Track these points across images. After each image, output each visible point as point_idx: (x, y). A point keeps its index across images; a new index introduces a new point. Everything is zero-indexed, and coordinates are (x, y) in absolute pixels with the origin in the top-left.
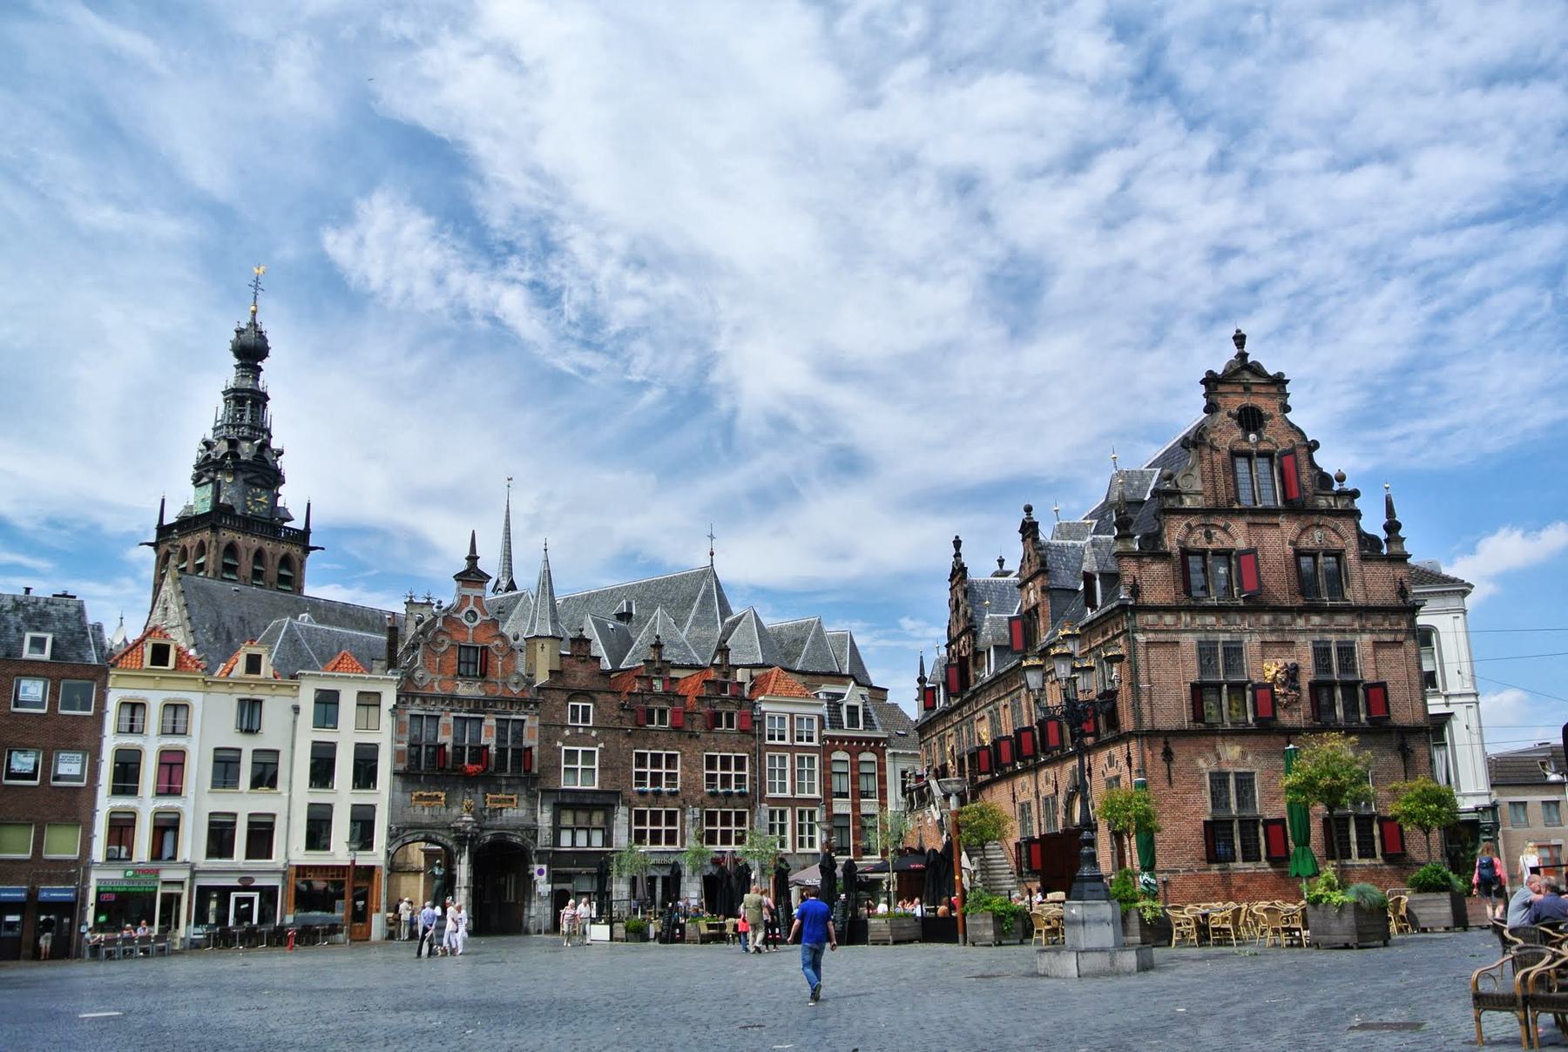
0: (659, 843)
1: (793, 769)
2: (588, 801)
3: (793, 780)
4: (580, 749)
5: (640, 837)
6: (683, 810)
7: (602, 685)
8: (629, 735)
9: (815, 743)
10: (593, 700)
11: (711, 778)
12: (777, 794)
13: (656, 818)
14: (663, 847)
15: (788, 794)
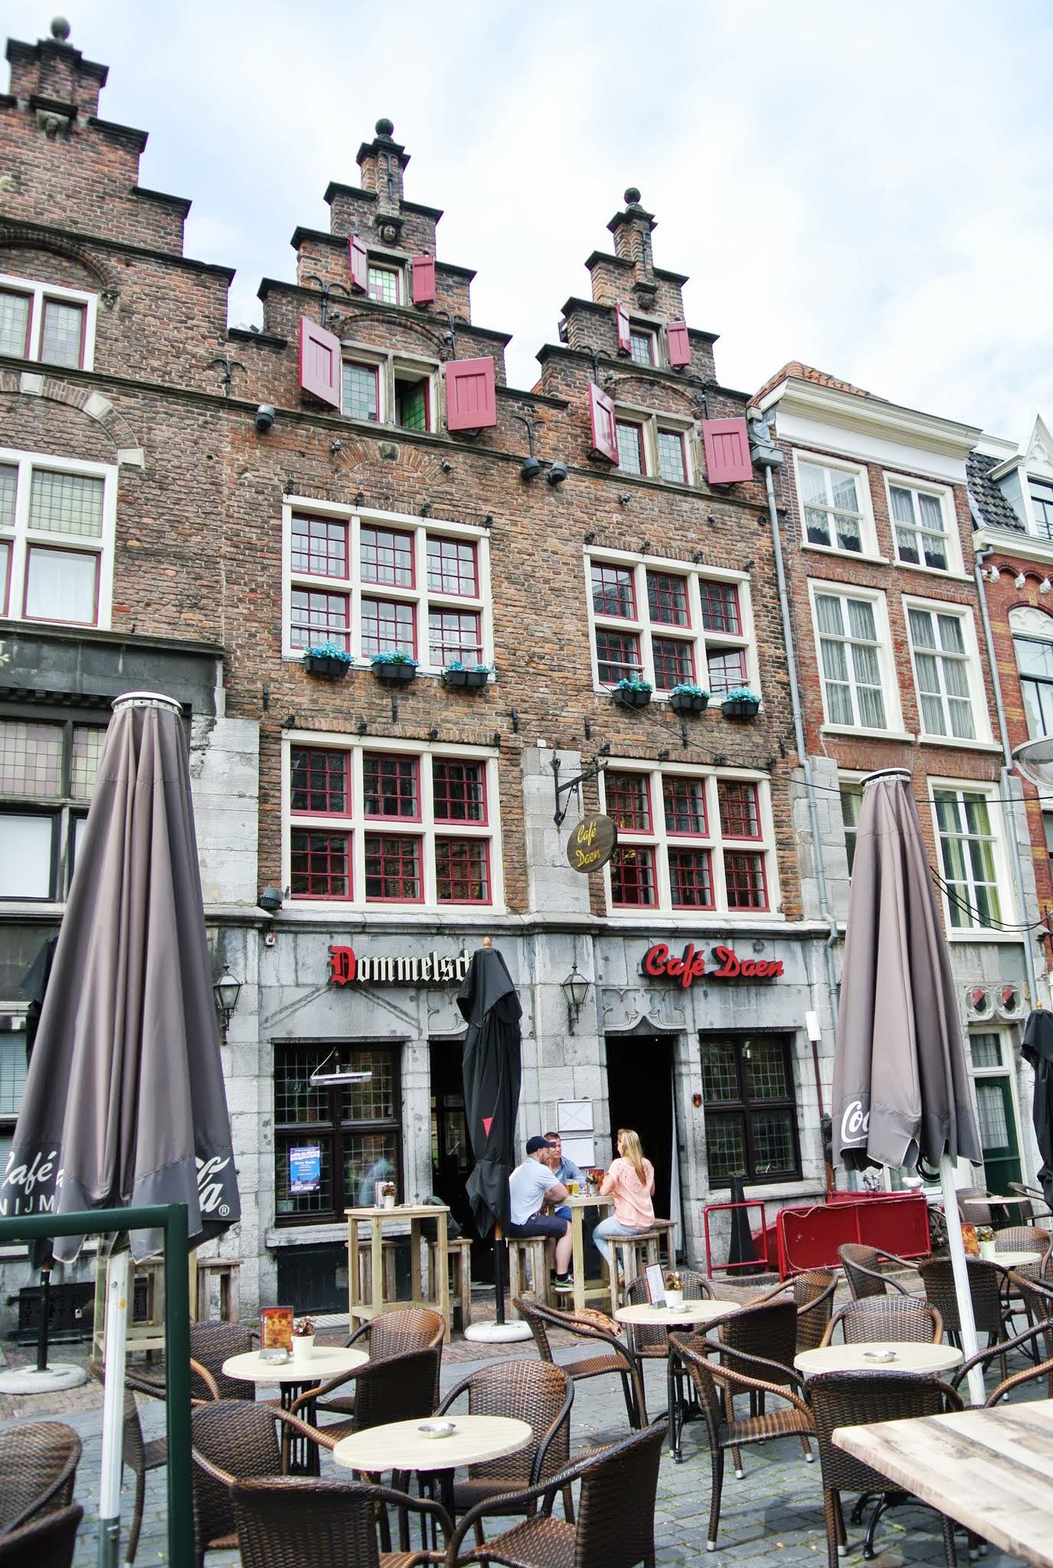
0: (410, 891)
1: (899, 645)
2: (53, 679)
3: (906, 684)
4: (26, 460)
5: (318, 864)
6: (512, 755)
7: (142, 236)
8: (263, 427)
9: (956, 568)
10: (97, 278)
11: (617, 644)
12: (858, 728)
13: (390, 781)
14: (430, 908)
15: (895, 728)
